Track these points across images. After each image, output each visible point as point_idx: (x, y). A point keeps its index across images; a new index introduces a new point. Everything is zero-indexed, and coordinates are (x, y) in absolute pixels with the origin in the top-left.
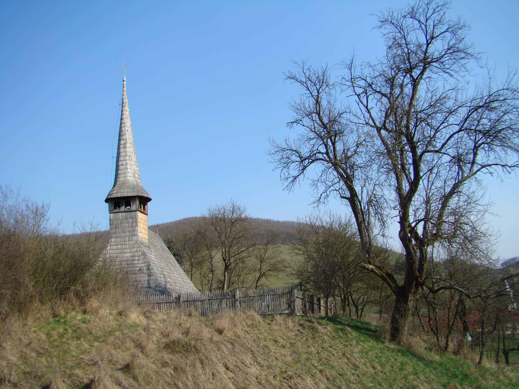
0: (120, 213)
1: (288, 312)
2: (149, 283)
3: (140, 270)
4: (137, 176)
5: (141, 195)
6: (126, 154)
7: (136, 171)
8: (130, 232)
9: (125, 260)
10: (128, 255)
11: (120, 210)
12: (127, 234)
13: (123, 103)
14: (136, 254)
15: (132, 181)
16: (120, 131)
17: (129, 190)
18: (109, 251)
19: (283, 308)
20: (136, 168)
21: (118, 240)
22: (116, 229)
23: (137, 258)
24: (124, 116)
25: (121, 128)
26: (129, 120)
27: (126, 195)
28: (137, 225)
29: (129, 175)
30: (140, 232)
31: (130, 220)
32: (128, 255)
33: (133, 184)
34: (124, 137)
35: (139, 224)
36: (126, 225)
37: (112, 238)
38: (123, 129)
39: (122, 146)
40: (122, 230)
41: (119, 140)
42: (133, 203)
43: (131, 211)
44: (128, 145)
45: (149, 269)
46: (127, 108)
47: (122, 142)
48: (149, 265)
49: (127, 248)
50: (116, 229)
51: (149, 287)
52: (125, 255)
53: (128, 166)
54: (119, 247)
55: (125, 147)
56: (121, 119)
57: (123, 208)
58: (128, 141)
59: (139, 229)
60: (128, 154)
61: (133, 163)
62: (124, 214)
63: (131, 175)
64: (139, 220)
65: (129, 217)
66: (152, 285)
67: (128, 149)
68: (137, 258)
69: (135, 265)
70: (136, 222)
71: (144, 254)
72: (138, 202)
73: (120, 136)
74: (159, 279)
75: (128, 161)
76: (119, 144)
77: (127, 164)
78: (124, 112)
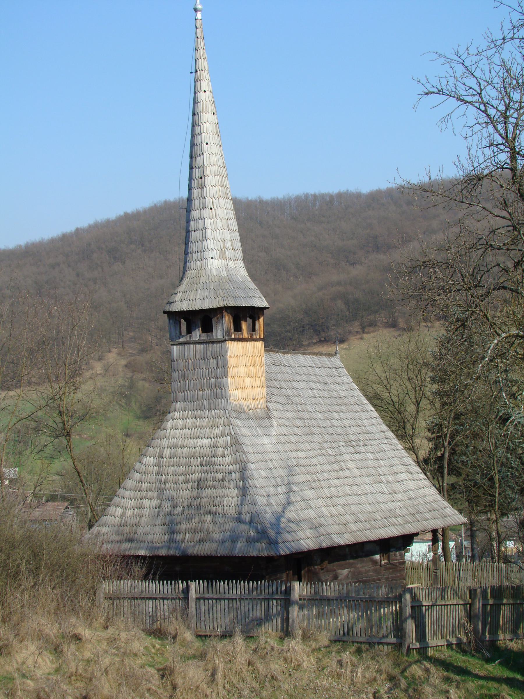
0: (192, 346)
1: (393, 640)
2: (240, 513)
3: (223, 480)
4: (229, 253)
5: (232, 303)
6: (204, 204)
7: (229, 244)
8: (211, 388)
9: (197, 454)
10: (205, 442)
11: (191, 337)
12: (207, 392)
13: (196, 71)
14: (221, 441)
15: (218, 270)
16: (193, 145)
17: (206, 293)
18: (169, 431)
19: (384, 632)
20: (227, 235)
21: (189, 405)
22: (184, 380)
23: (220, 451)
24: (200, 106)
25: (193, 136)
26: (210, 115)
27: (198, 306)
28: (225, 374)
29: (211, 254)
30: (237, 388)
31: (212, 362)
32: (205, 442)
33: (219, 277)
34: (198, 161)
35: (231, 371)
36: (203, 372)
37: (176, 400)
38: (197, 139)
39: (195, 184)
40: (195, 385)
41: (191, 168)
42: (217, 323)
43: (213, 342)
44: (209, 181)
45: (243, 479)
46: (204, 85)
47: (197, 173)
48: (243, 470)
49: (205, 425)
50: (184, 380)
51: (239, 520)
52: (200, 442)
53: (209, 233)
54: (189, 422)
55: (202, 187)
56: (194, 114)
57: (197, 334)
58: (208, 171)
59: (231, 382)
60: (209, 202)
61: (219, 225)
62: (200, 347)
63: (216, 254)
64: (231, 361)
65: (209, 353)
66: (243, 516)
67: (209, 191)
68: (220, 451)
69: (216, 467)
70: (224, 365)
71: (236, 443)
72: (227, 320)
73: (191, 157)
74: (261, 501)
75: (207, 222)
76: (191, 179)
77: (205, 228)
78: (201, 96)
